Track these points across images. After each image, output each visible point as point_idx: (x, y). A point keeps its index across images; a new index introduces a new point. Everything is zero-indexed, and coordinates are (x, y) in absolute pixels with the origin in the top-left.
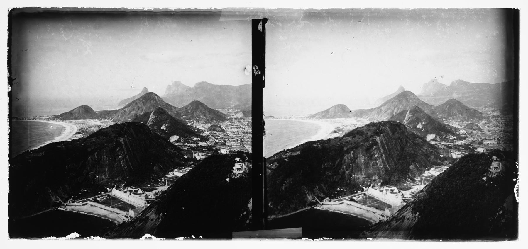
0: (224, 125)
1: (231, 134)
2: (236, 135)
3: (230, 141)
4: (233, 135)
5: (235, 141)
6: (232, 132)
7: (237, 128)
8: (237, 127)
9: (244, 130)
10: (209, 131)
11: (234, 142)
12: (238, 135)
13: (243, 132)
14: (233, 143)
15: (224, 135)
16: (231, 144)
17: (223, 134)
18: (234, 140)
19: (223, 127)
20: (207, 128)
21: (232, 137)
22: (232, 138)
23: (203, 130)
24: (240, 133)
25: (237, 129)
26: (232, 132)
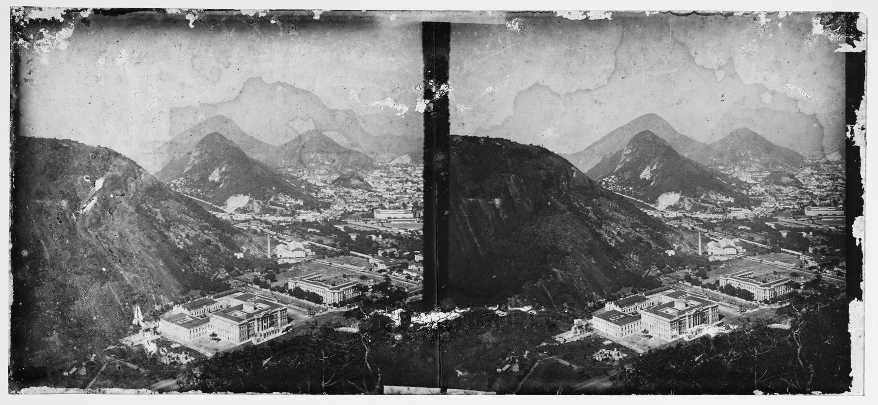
0: (370, 178)
1: (388, 192)
2: (400, 196)
3: (384, 208)
4: (392, 195)
5: (399, 208)
6: (388, 190)
7: (401, 182)
8: (399, 180)
9: (416, 184)
10: (766, 184)
11: (827, 209)
12: (406, 194)
13: (415, 188)
14: (392, 213)
15: (801, 193)
16: (820, 213)
17: (797, 191)
18: (397, 204)
19: (369, 180)
20: (761, 180)
21: (822, 195)
22: (390, 202)
23: (749, 184)
24: (408, 191)
25: (402, 184)
26: (388, 190)
